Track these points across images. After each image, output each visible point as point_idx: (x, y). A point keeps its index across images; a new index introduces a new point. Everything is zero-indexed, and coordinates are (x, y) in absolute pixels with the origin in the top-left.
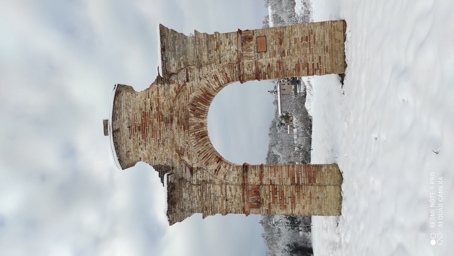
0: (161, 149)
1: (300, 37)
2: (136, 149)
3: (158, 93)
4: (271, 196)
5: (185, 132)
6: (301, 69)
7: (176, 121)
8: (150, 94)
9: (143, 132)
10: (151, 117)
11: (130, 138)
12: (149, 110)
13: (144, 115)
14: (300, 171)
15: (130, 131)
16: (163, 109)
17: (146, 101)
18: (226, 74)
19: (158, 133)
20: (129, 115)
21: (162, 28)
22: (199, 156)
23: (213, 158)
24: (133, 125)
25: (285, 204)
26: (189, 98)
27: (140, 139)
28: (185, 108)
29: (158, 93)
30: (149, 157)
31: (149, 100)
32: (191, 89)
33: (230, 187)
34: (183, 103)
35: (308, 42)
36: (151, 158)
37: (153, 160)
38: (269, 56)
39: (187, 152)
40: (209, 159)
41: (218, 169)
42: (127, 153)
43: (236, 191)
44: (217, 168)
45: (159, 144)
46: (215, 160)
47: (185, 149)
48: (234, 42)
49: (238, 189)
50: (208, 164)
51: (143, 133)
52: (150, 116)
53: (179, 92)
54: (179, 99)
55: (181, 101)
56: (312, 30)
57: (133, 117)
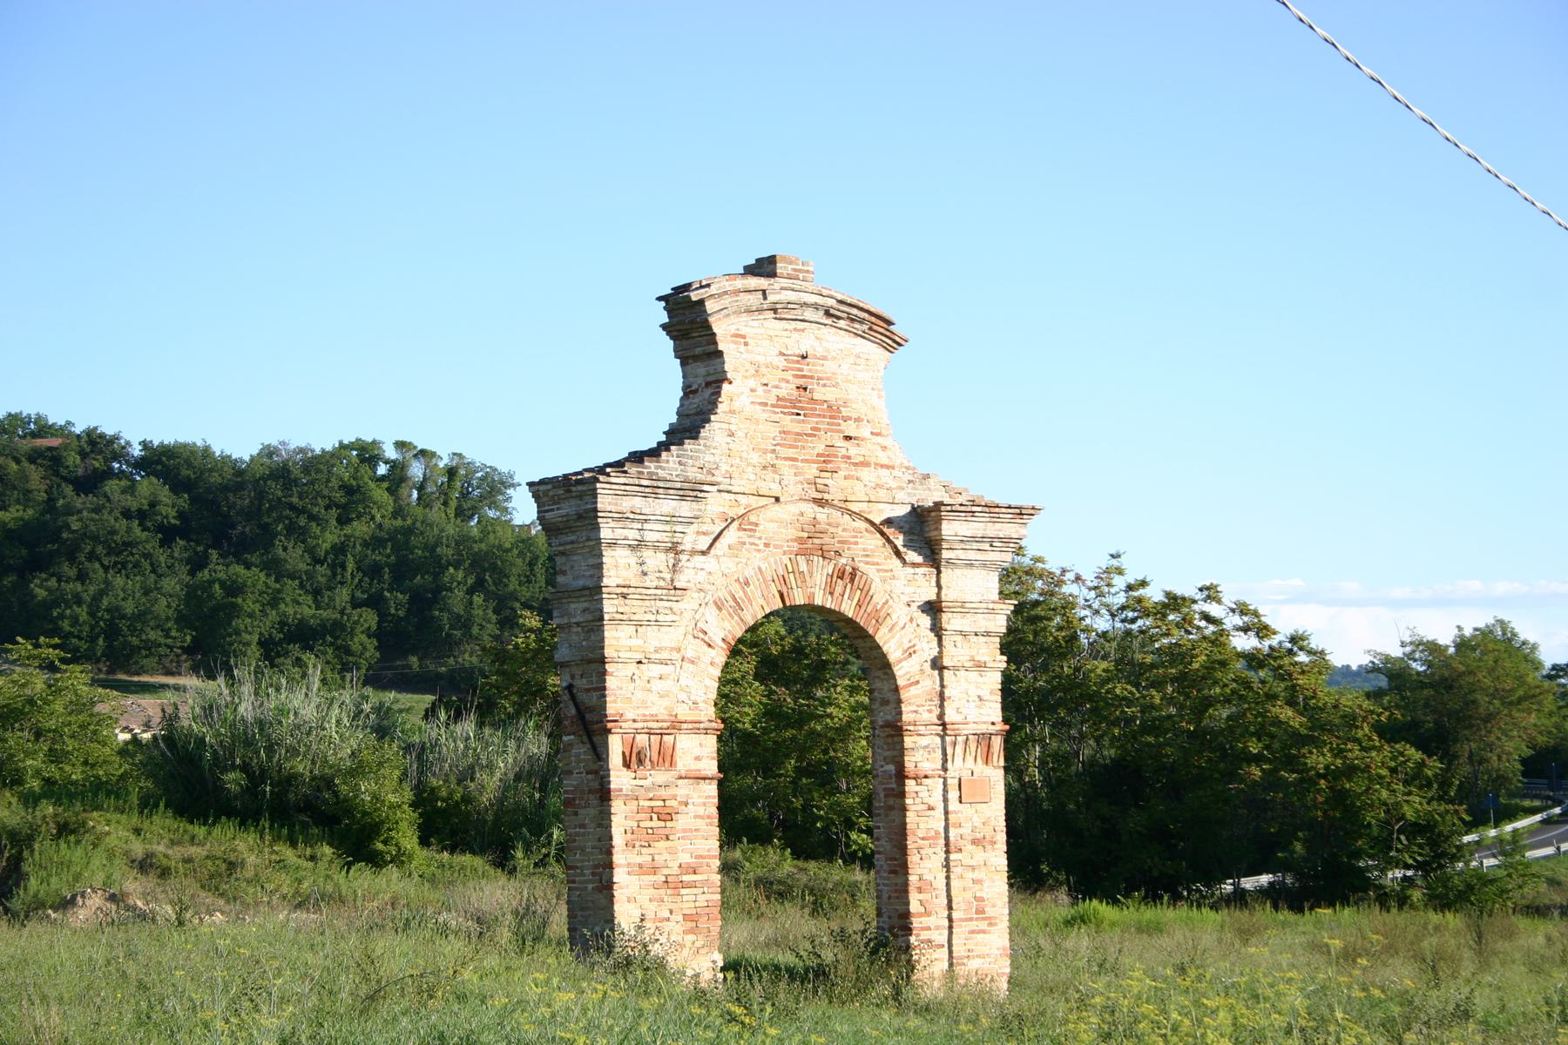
0: (755, 458)
1: (984, 895)
5: (792, 540)
8: (879, 439)
9: (793, 403)
10: (829, 434)
11: (782, 354)
12: (842, 432)
13: (833, 412)
14: (710, 890)
15: (795, 358)
17: (865, 422)
18: (918, 682)
19: (791, 453)
21: (1034, 510)
23: (733, 627)
24: (810, 370)
25: (637, 844)
26: (867, 563)
27: (777, 387)
28: (846, 546)
30: (732, 412)
31: (864, 432)
32: (886, 571)
33: (669, 675)
34: (856, 543)
35: (975, 916)
36: (733, 420)
37: (726, 426)
39: (744, 543)
40: (730, 614)
41: (706, 639)
42: (743, 337)
43: (662, 697)
44: (710, 638)
45: (765, 452)
46: (729, 631)
47: (751, 536)
48: (981, 711)
49: (666, 702)
50: (720, 609)
51: (791, 401)
54: (866, 530)
55: (861, 537)
56: (996, 924)
57: (829, 375)
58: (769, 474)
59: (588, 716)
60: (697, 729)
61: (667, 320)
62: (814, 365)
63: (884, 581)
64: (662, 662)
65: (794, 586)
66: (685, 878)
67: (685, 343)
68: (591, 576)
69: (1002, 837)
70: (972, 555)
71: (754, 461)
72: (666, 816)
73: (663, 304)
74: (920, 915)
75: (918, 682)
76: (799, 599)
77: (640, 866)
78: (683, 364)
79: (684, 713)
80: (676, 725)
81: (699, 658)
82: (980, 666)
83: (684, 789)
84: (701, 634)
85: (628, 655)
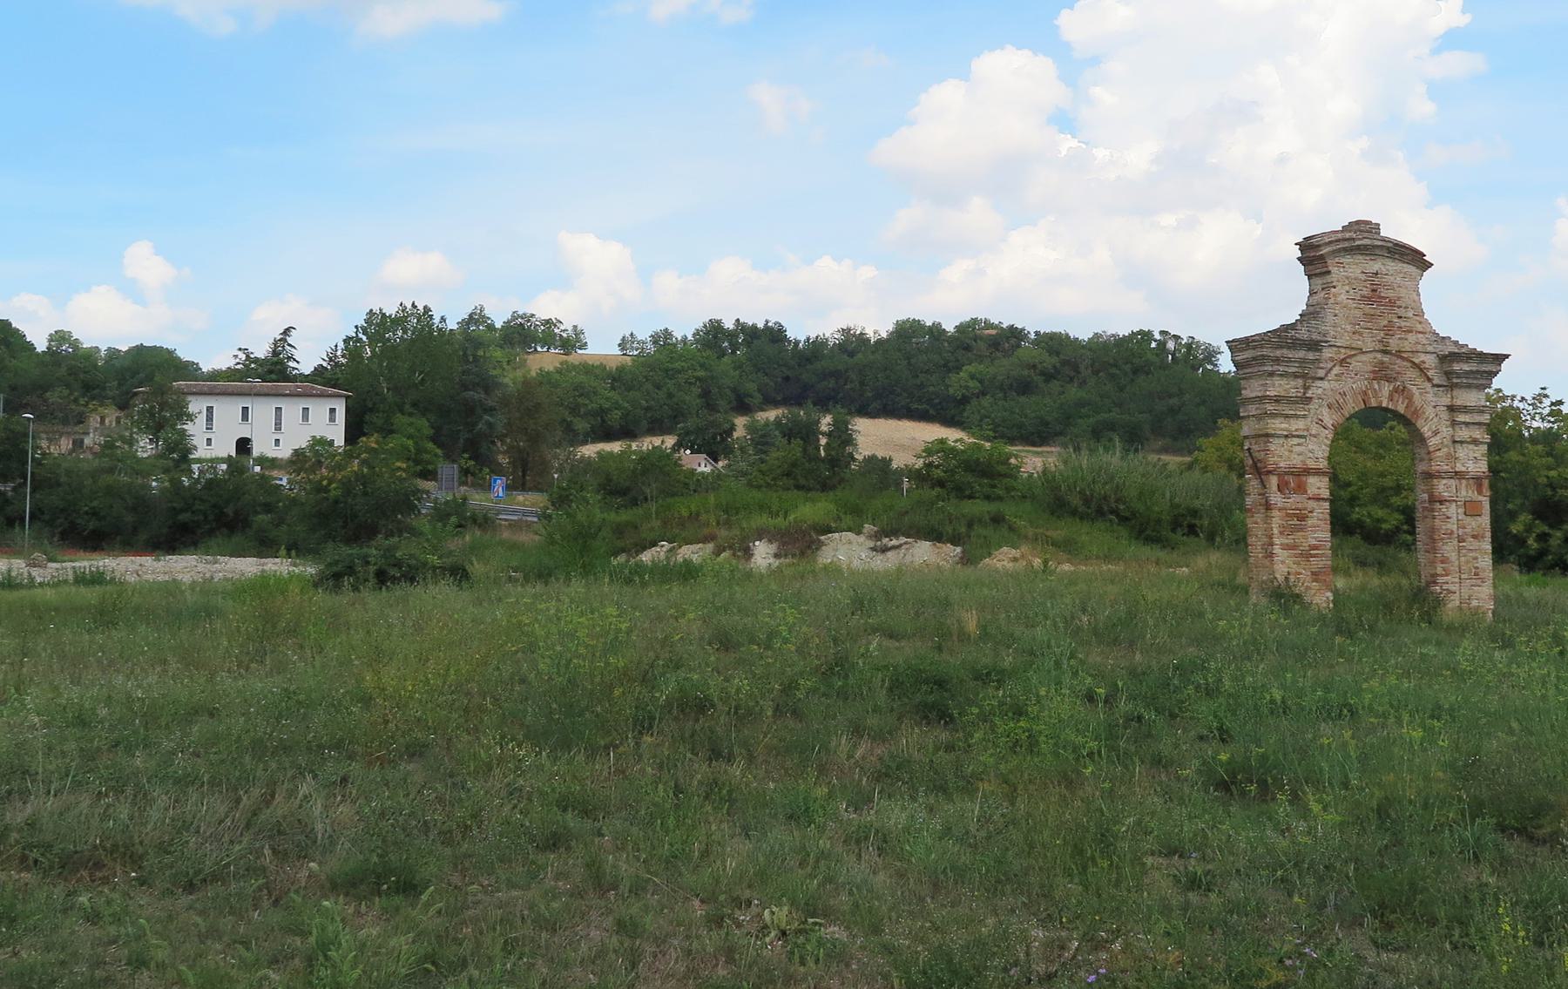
0: (1349, 328)
2: (1347, 282)
3: (1420, 332)
4: (1294, 512)
6: (1443, 565)
7: (1385, 359)
8: (1418, 318)
9: (1369, 299)
12: (1396, 314)
13: (1392, 303)
16: (1399, 339)
18: (1440, 449)
20: (1392, 275)
22: (1340, 393)
26: (1411, 385)
27: (1361, 290)
29: (1420, 332)
38: (1460, 518)
39: (1343, 373)
43: (1299, 455)
45: (1355, 325)
50: (1329, 408)
51: (1368, 298)
52: (1391, 313)
53: (1421, 370)
58: (1356, 337)
59: (1259, 465)
60: (1318, 472)
61: (1300, 255)
62: (1381, 278)
63: (1421, 394)
64: (1298, 436)
65: (1371, 396)
66: (1312, 552)
67: (1310, 267)
68: (1260, 390)
69: (1488, 534)
70: (1471, 381)
71: (1348, 330)
72: (1302, 518)
73: (1298, 246)
74: (1442, 575)
75: (1440, 449)
76: (1374, 403)
77: (1287, 545)
78: (1309, 279)
79: (1311, 464)
80: (1307, 471)
81: (1319, 434)
82: (1475, 442)
83: (1311, 504)
84: (1320, 422)
85: (1280, 432)
